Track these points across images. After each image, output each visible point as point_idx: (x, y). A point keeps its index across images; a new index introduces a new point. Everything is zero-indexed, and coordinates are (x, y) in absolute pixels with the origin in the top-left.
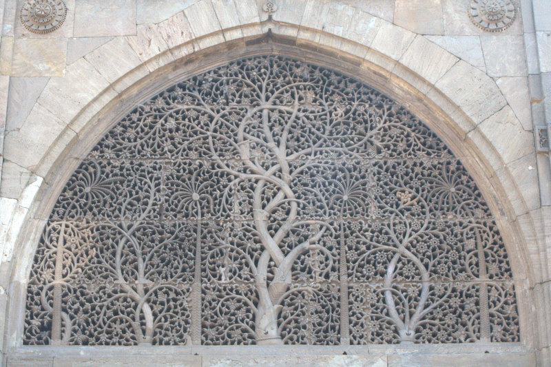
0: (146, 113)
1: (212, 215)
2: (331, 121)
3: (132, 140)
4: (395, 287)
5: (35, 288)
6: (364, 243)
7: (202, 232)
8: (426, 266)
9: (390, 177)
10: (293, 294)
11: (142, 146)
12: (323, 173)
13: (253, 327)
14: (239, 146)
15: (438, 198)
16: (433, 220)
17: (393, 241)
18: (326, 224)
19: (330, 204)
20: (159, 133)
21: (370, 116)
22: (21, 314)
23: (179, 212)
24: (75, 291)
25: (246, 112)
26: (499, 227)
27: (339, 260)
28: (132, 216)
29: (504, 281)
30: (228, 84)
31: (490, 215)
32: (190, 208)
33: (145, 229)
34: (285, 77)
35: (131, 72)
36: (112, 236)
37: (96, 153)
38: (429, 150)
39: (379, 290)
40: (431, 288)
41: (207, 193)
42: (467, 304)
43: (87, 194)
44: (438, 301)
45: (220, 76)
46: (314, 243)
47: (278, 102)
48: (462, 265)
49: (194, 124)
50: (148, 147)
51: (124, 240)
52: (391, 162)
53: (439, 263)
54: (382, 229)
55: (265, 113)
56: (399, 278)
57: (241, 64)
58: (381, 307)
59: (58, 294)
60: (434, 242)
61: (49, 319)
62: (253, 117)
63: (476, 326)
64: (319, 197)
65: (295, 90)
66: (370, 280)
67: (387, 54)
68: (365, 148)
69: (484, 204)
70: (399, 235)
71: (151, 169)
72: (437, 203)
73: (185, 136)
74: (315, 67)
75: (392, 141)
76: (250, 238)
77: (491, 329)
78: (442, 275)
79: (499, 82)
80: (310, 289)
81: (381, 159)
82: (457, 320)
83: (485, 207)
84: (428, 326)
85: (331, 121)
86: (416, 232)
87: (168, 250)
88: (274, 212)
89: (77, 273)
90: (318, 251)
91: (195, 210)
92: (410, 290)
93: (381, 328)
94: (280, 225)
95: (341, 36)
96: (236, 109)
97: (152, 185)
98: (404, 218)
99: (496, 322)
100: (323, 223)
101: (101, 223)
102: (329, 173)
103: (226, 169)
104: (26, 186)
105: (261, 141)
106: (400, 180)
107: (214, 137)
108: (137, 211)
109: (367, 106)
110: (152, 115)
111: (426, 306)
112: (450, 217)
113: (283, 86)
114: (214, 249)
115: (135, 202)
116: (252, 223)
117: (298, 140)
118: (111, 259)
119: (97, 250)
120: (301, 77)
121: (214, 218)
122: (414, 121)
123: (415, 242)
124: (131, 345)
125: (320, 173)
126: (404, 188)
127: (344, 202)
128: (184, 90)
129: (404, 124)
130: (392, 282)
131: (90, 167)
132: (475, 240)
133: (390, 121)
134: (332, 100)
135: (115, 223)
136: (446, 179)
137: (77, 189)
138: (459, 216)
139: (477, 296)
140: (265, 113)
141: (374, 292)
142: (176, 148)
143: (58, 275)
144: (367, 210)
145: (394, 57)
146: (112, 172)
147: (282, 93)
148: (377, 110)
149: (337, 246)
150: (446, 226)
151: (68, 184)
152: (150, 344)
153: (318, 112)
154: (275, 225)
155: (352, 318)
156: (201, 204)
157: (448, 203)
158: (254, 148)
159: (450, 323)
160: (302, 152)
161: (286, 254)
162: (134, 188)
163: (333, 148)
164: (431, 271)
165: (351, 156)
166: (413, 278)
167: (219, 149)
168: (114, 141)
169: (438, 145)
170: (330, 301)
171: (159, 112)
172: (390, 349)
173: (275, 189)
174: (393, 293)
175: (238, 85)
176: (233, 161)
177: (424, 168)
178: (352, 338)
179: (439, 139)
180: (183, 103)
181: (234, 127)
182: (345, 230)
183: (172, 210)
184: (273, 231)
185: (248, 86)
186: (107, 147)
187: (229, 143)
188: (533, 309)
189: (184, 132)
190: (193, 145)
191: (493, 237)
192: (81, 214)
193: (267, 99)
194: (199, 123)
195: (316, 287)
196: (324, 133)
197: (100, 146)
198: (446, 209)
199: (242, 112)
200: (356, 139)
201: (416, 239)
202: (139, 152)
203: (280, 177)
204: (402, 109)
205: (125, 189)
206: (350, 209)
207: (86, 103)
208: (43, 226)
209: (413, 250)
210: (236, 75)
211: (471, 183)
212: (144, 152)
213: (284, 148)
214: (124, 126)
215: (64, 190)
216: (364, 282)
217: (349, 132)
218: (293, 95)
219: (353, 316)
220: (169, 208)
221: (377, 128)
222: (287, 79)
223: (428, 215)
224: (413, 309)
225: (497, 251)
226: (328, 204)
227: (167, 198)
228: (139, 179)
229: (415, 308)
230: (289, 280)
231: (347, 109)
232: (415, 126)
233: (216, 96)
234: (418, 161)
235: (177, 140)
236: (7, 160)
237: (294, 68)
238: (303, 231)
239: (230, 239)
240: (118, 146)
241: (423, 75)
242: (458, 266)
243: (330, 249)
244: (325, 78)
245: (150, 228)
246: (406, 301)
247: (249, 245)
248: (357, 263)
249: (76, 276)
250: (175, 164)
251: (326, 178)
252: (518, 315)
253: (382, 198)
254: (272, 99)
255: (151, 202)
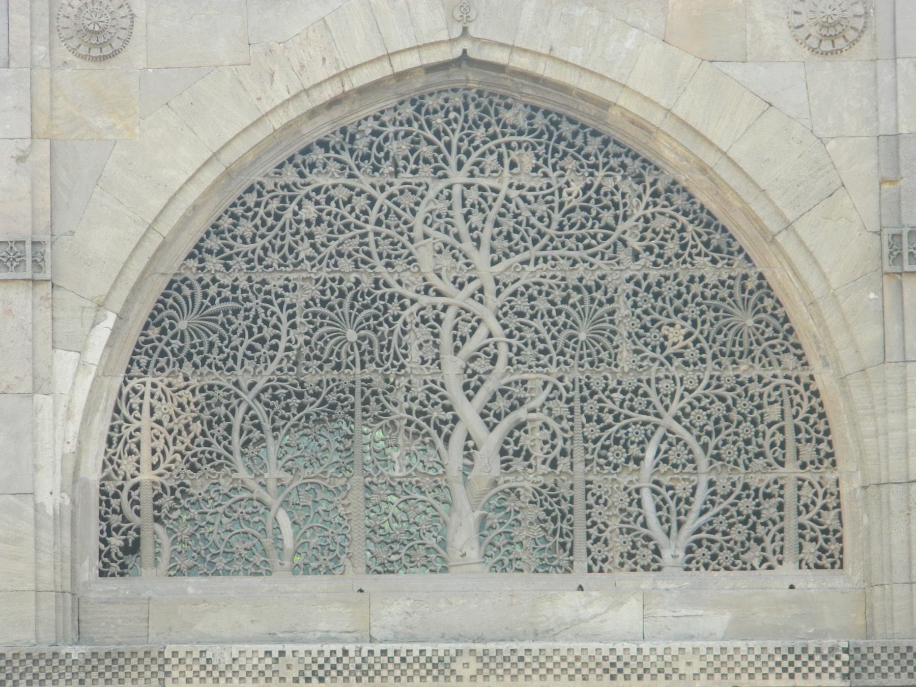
0: (268, 192)
1: (378, 365)
2: (562, 205)
3: (248, 240)
4: (657, 482)
5: (111, 488)
6: (611, 411)
7: (363, 393)
8: (705, 447)
9: (653, 300)
10: (503, 491)
11: (264, 249)
12: (548, 294)
13: (443, 543)
14: (417, 248)
15: (726, 336)
16: (717, 374)
17: (655, 408)
18: (553, 380)
19: (560, 346)
20: (291, 228)
21: (623, 195)
22: (94, 528)
23: (328, 361)
24: (173, 490)
25: (427, 189)
26: (817, 385)
27: (572, 438)
28: (255, 368)
29: (824, 472)
30: (396, 139)
31: (806, 364)
32: (343, 355)
33: (275, 388)
34: (488, 125)
35: (246, 130)
36: (225, 401)
37: (193, 263)
38: (717, 256)
39: (632, 487)
40: (711, 483)
41: (369, 328)
42: (764, 508)
43: (182, 333)
44: (720, 503)
45: (383, 124)
46: (534, 411)
47: (477, 170)
48: (760, 446)
49: (345, 211)
50: (274, 251)
51: (243, 408)
52: (654, 275)
53: (725, 442)
54: (638, 388)
55: (457, 191)
56: (663, 468)
57: (418, 104)
58: (634, 514)
59: (146, 496)
60: (718, 409)
61: (136, 535)
62: (437, 198)
63: (777, 544)
64: (540, 335)
65: (503, 149)
66: (619, 470)
67: (655, 99)
68: (615, 252)
69: (797, 346)
70: (664, 398)
71: (280, 291)
72: (724, 344)
73: (332, 232)
74: (535, 109)
75: (657, 240)
76: (436, 404)
77: (801, 548)
78: (729, 462)
79: (831, 145)
80: (528, 485)
81: (638, 270)
82: (749, 534)
83: (799, 352)
84: (705, 543)
85: (562, 205)
86: (691, 392)
87: (311, 424)
88: (473, 359)
89: (173, 461)
90: (539, 423)
91: (351, 358)
92: (679, 486)
93: (634, 547)
94: (482, 381)
95: (579, 64)
96: (410, 184)
97: (284, 317)
98: (672, 369)
99: (808, 537)
100: (546, 378)
101: (207, 381)
102: (557, 295)
103: (397, 289)
104: (93, 326)
105: (450, 240)
106: (668, 306)
107: (377, 234)
108: (262, 359)
109: (619, 178)
110: (277, 196)
111: (703, 512)
112: (743, 368)
113: (484, 143)
114: (381, 420)
115: (258, 345)
116: (439, 379)
117: (509, 238)
118: (225, 438)
119: (202, 424)
120: (513, 127)
121: (381, 370)
122: (693, 203)
123: (688, 409)
124: (261, 574)
125: (544, 294)
126: (674, 319)
127: (580, 343)
128: (327, 151)
129: (677, 210)
130: (653, 474)
131: (184, 287)
132: (782, 405)
133: (655, 205)
134: (563, 169)
135: (229, 380)
136: (740, 303)
137: (166, 323)
138: (757, 366)
139: (781, 496)
140: (457, 191)
141: (625, 488)
142: (319, 253)
143: (145, 466)
144: (616, 354)
145: (663, 103)
146: (219, 294)
147: (483, 155)
148: (635, 186)
149: (570, 416)
150: (738, 383)
151: (152, 316)
152: (290, 573)
153: (541, 189)
154: (474, 381)
155: (591, 531)
156: (359, 346)
157: (741, 344)
158: (440, 252)
159: (739, 538)
160: (515, 259)
161: (491, 428)
162: (254, 321)
163: (564, 252)
164: (712, 456)
165: (591, 265)
166: (684, 466)
167: (385, 255)
168: (220, 242)
169: (729, 245)
170: (558, 503)
171: (290, 190)
172: (647, 580)
173: (474, 323)
174: (654, 491)
175: (413, 142)
176: (408, 274)
177: (706, 286)
178: (591, 562)
179: (731, 236)
180: (327, 173)
181: (407, 216)
182: (581, 390)
183: (317, 358)
184: (471, 392)
185: (430, 142)
186: (209, 251)
187: (400, 245)
188: (866, 520)
189: (330, 225)
190: (345, 249)
191: (810, 399)
192: (174, 367)
193: (460, 165)
194: (353, 210)
195: (537, 482)
196: (548, 226)
197: (198, 252)
198: (737, 354)
199: (421, 190)
200: (600, 236)
201: (690, 404)
202: (261, 260)
203: (481, 301)
204: (674, 183)
205: (240, 323)
206: (589, 355)
207: (177, 188)
208: (118, 386)
209: (686, 422)
210: (409, 123)
211: (779, 312)
212: (268, 261)
213: (488, 251)
214: (234, 216)
215: (146, 326)
216: (609, 473)
217: (589, 224)
218: (500, 159)
219: (591, 527)
220: (312, 355)
221: (635, 217)
222: (491, 130)
223: (710, 364)
224: (682, 518)
225: (815, 423)
226: (555, 346)
227: (308, 338)
228: (263, 307)
229: (686, 515)
230: (496, 468)
231: (586, 184)
232: (695, 212)
233: (378, 160)
234: (697, 274)
235: (319, 239)
236: (58, 286)
237: (502, 109)
238: (518, 391)
239: (406, 405)
240: (228, 252)
241: (709, 137)
242: (753, 449)
243: (559, 419)
244: (552, 128)
245: (283, 387)
246: (672, 504)
247: (435, 414)
248: (599, 444)
249: (173, 466)
250: (317, 281)
251: (553, 303)
252: (842, 526)
253: (639, 337)
254: (467, 167)
255: (282, 344)
